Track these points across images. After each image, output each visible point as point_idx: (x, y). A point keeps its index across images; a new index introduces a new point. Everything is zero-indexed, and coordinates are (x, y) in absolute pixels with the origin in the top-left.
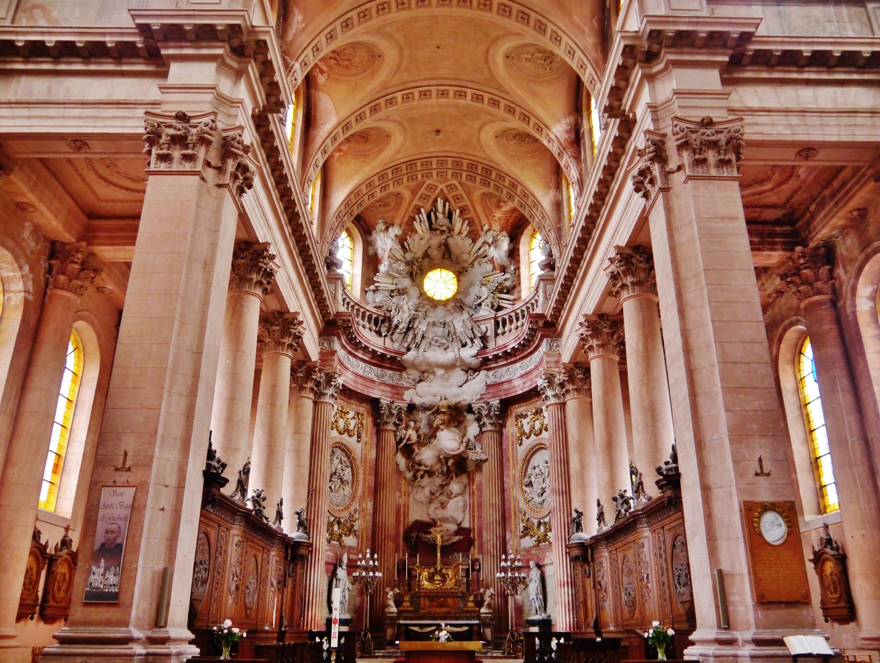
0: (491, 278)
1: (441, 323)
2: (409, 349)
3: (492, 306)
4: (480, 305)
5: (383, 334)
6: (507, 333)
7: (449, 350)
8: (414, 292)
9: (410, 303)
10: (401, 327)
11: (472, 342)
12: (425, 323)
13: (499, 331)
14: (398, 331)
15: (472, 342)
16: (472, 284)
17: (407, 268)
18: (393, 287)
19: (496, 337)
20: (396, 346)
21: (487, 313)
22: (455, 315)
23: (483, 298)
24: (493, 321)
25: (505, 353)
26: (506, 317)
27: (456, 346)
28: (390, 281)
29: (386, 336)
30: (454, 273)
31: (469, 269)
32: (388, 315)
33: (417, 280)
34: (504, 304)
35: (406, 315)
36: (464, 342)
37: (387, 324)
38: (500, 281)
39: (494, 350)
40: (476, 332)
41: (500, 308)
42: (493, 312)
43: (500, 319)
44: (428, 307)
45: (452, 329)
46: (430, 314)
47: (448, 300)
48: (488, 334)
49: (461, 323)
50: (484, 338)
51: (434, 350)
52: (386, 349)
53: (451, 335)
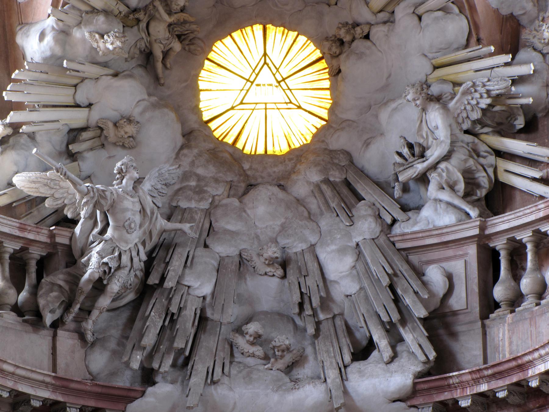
0: (464, 71)
1: (271, 262)
2: (148, 377)
3: (471, 183)
4: (423, 179)
5: (49, 319)
6: (528, 303)
7: (307, 370)
8: (160, 135)
9: (147, 186)
10: (115, 287)
11: (396, 340)
12: (206, 261)
13: (499, 292)
14: (104, 302)
15: (396, 340)
16: (386, 94)
17: (133, 35)
18: (77, 118)
19: (484, 316)
20: (99, 360)
21: (448, 219)
22: (325, 223)
23: (433, 154)
24: (472, 251)
25: (521, 386)
26: (525, 236)
27: (328, 355)
28: (63, 95)
29: (55, 325)
30: (318, 40)
31: (378, 32)
32: (62, 239)
33: (173, 78)
34: (520, 178)
35: (135, 237)
36: (361, 335)
37: (59, 278)
38: (497, 88)
39: (478, 376)
40: (408, 300)
41: (499, 198)
42: (474, 213)
43: (500, 244)
44: (219, 190)
45: (312, 282)
46: (227, 223)
47: (297, 156)
48: (457, 302)
49: (349, 260)
50: (439, 324)
51: (248, 378)
52: (62, 384)
53: (313, 308)
